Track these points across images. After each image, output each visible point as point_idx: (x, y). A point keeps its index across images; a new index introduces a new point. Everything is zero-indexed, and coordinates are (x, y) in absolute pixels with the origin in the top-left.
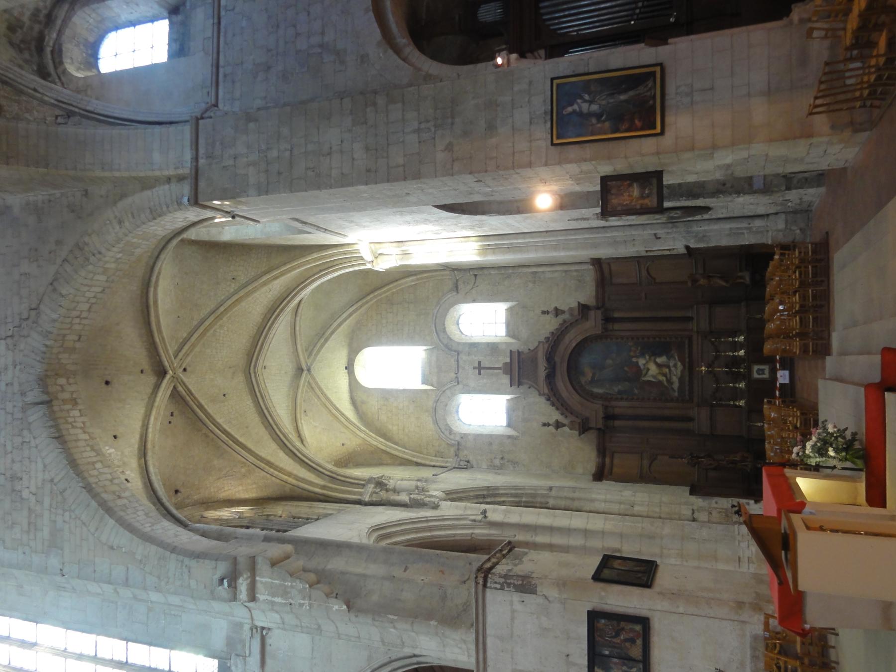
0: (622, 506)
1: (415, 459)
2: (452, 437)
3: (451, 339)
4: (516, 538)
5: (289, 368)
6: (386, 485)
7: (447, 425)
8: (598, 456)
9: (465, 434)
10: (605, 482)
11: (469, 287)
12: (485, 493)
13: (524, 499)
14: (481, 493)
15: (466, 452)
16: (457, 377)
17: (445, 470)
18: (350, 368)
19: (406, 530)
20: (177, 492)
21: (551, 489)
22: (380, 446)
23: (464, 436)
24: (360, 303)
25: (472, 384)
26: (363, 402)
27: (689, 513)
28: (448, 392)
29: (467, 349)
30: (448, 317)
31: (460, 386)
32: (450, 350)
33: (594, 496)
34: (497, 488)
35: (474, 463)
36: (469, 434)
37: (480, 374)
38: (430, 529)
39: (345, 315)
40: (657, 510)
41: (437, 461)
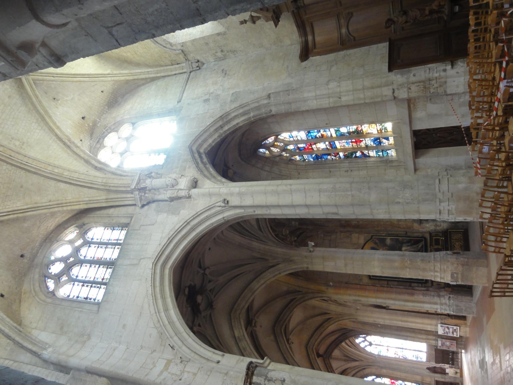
0: (331, 100)
2: (174, 48)
4: (256, 213)
6: (146, 188)
8: (301, 36)
9: (183, 43)
10: (311, 58)
12: (221, 123)
13: (252, 115)
14: (218, 125)
15: (192, 55)
19: (176, 243)
20: (22, 256)
21: (269, 96)
22: (127, 78)
23: (183, 44)
27: (390, 93)
33: (306, 95)
34: (228, 114)
35: (203, 60)
36: (186, 42)
38: (193, 229)
40: (362, 96)
41: (176, 69)
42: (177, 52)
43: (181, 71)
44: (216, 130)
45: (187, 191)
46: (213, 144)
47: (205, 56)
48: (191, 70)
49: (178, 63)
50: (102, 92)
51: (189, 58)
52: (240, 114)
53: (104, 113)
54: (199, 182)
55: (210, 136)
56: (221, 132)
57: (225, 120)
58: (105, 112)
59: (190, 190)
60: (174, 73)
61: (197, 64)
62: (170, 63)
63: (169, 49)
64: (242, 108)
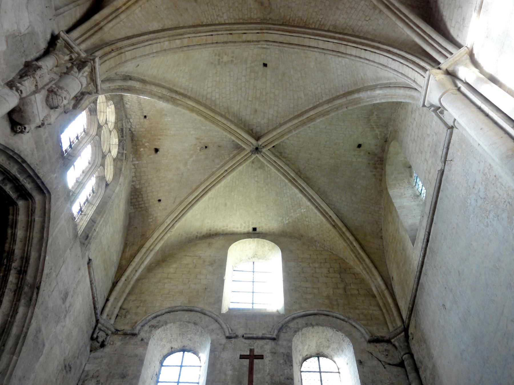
1: (123, 279)
2: (146, 328)
3: (296, 332)
5: (260, 121)
6: (80, 69)
7: (166, 323)
11: (382, 358)
12: (29, 278)
14: (31, 271)
15: (118, 344)
16: (236, 337)
17: (99, 313)
18: (255, 233)
22: (151, 241)
23: (144, 343)
24: (340, 224)
25: (226, 355)
26: (210, 244)
28: (215, 326)
29: (282, 350)
30: (329, 333)
31: (224, 341)
32: (280, 330)
34: (31, 303)
35: (99, 353)
37: (242, 357)
39: (323, 205)
42: (138, 328)
43: (107, 310)
44: (25, 259)
45: (24, 95)
46: (9, 231)
47: (105, 361)
48: (99, 325)
49: (119, 318)
50: (160, 200)
51: (116, 336)
52: (11, 323)
53: (135, 176)
54: (8, 129)
55: (27, 241)
56: (15, 265)
57: (26, 289)
58: (135, 179)
59: (22, 99)
60: (112, 299)
61: (100, 340)
62: (125, 307)
63: (149, 321)
64: (18, 337)
